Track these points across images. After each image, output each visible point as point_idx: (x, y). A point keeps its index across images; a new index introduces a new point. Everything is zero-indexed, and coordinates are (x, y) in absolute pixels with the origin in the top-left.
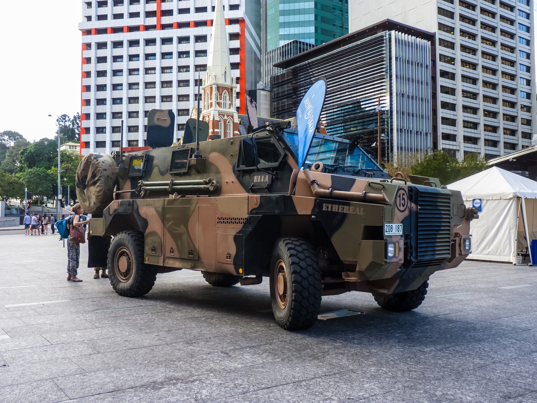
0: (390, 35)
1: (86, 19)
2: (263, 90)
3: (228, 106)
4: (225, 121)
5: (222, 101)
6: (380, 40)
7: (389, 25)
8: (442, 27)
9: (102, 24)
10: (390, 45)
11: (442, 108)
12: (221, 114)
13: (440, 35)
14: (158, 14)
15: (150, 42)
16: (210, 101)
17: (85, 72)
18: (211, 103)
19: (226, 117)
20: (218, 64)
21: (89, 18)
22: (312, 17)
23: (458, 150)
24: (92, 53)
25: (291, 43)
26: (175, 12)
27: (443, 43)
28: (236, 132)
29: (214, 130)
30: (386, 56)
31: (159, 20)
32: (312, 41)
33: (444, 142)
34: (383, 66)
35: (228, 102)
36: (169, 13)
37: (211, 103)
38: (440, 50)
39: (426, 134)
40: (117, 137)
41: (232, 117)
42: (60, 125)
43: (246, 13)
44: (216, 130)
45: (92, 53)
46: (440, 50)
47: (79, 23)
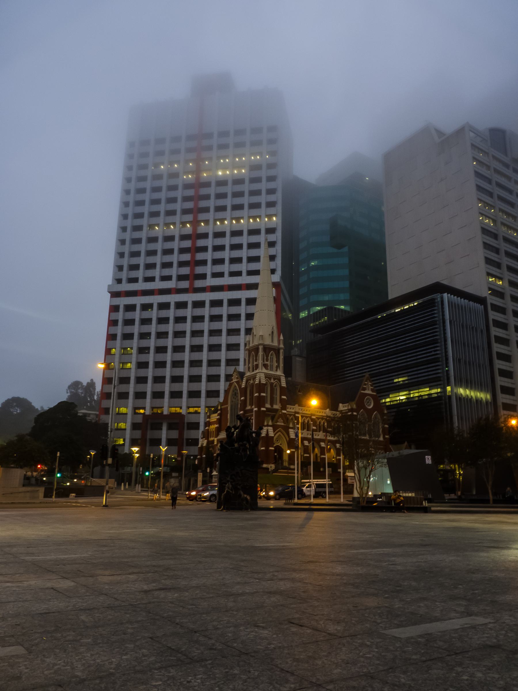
0: (442, 298)
1: (116, 282)
3: (275, 369)
5: (268, 363)
7: (438, 288)
10: (443, 308)
12: (268, 377)
13: (492, 300)
17: (111, 334)
19: (272, 381)
20: (265, 325)
21: (119, 281)
24: (120, 316)
25: (325, 309)
29: (260, 394)
31: (192, 284)
34: (436, 330)
35: (275, 364)
36: (203, 276)
41: (279, 380)
42: (71, 392)
43: (283, 277)
45: (120, 316)
46: (493, 315)
47: (109, 286)
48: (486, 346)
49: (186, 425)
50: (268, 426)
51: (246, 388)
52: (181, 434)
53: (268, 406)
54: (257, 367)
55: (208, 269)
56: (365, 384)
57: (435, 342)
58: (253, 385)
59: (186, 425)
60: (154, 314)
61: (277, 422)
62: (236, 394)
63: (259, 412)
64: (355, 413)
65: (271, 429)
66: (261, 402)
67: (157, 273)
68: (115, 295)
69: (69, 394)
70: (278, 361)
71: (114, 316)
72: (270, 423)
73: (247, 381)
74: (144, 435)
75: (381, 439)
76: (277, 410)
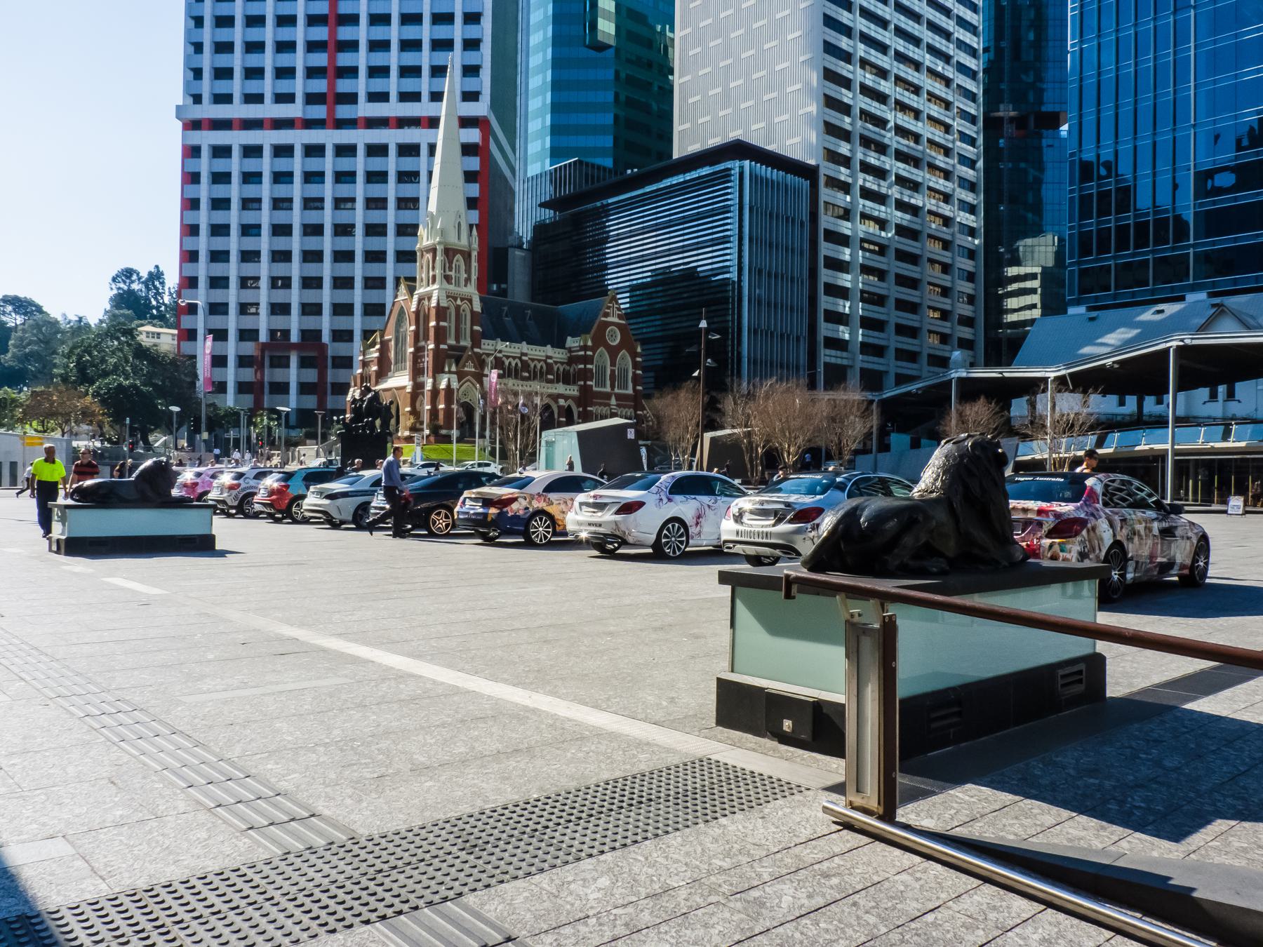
0: (742, 168)
1: (191, 100)
3: (463, 282)
4: (458, 308)
5: (452, 273)
6: (725, 176)
7: (739, 149)
9: (222, 112)
11: (826, 294)
13: (827, 169)
14: (330, 99)
15: (314, 151)
16: (431, 273)
18: (434, 277)
19: (459, 302)
21: (197, 99)
22: (609, 119)
27: (834, 183)
28: (477, 328)
31: (331, 111)
32: (608, 162)
33: (828, 352)
36: (351, 98)
37: (434, 277)
38: (826, 194)
39: (798, 339)
40: (248, 322)
41: (470, 301)
44: (442, 324)
45: (204, 165)
47: (178, 107)
48: (806, 246)
50: (450, 372)
52: (322, 375)
53: (452, 342)
55: (361, 85)
56: (609, 308)
60: (266, 165)
61: (464, 366)
63: (437, 351)
64: (589, 353)
65: (454, 377)
67: (268, 85)
69: (115, 292)
70: (468, 271)
71: (192, 165)
72: (454, 368)
73: (420, 300)
75: (630, 391)
76: (464, 349)
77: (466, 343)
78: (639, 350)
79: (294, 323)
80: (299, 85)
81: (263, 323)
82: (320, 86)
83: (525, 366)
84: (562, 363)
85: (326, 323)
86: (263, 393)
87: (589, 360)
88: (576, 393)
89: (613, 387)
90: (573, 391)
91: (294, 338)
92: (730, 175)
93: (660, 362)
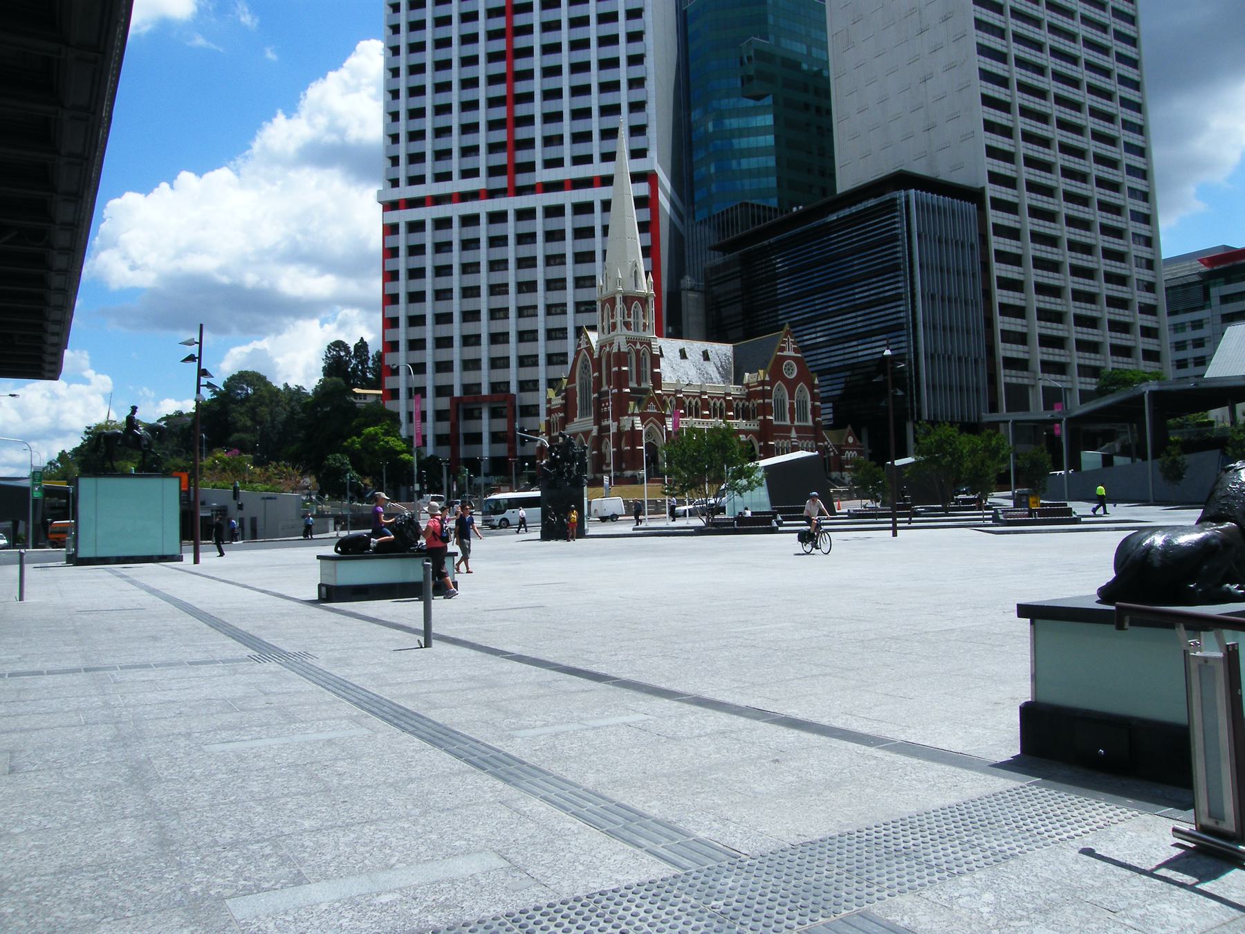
0: (907, 197)
2: (692, 289)
5: (631, 320)
7: (903, 180)
8: (995, 178)
13: (993, 191)
15: (498, 217)
19: (638, 346)
21: (395, 183)
23: (1033, 386)
24: (402, 240)
26: (539, 165)
27: (998, 204)
30: (901, 228)
32: (773, 203)
36: (530, 167)
39: (976, 361)
40: (443, 379)
41: (649, 345)
45: (402, 240)
46: (994, 217)
48: (978, 267)
49: (518, 409)
50: (633, 414)
51: (600, 358)
53: (633, 384)
54: (614, 327)
55: (538, 154)
56: (784, 342)
57: (896, 268)
58: (609, 354)
59: (518, 409)
61: (646, 408)
62: (586, 367)
65: (638, 420)
66: (621, 379)
67: (455, 164)
68: (390, 206)
72: (637, 411)
74: (454, 427)
75: (810, 423)
76: (646, 391)
77: (649, 384)
78: (816, 382)
79: (484, 377)
80: (482, 161)
81: (456, 379)
82: (501, 159)
83: (705, 404)
84: (741, 399)
85: (513, 375)
86: (458, 444)
87: (767, 394)
88: (756, 428)
89: (792, 420)
90: (753, 425)
91: (485, 391)
92: (896, 205)
93: (839, 392)
